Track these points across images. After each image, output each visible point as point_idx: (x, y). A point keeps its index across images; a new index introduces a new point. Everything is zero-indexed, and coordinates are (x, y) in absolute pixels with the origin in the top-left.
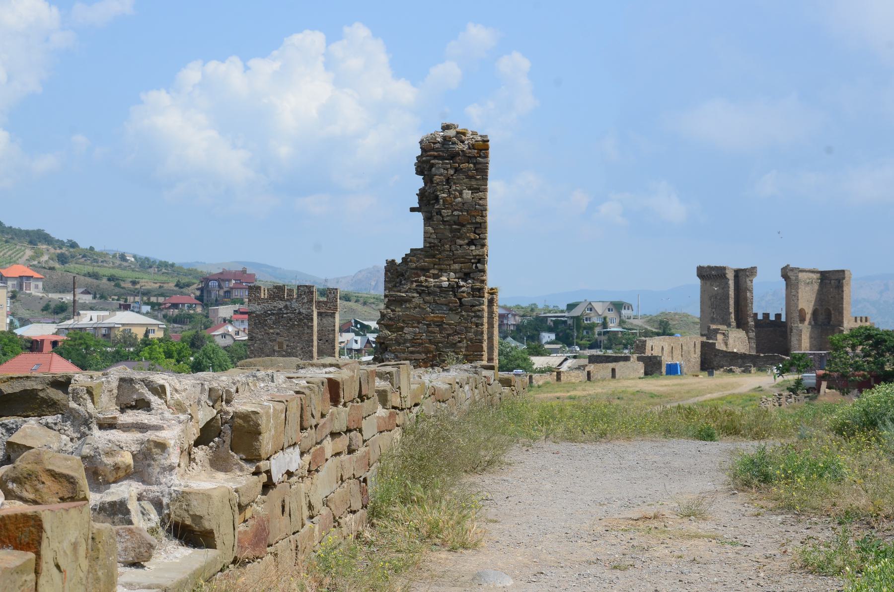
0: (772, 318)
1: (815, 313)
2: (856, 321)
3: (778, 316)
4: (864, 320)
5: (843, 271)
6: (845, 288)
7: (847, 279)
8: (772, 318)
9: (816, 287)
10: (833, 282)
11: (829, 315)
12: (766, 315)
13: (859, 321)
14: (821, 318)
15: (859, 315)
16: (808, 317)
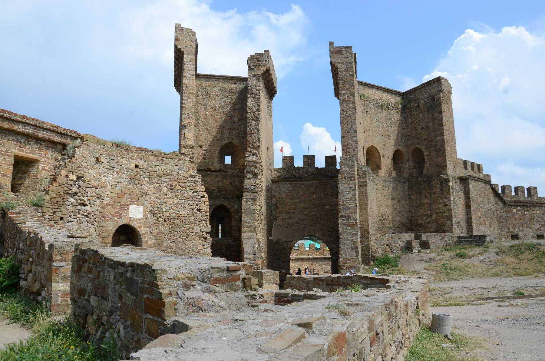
0: (320, 163)
1: (397, 157)
2: (466, 167)
3: (330, 160)
4: (476, 169)
5: (438, 79)
6: (444, 108)
7: (445, 92)
8: (320, 163)
9: (396, 116)
10: (421, 102)
11: (419, 157)
12: (309, 160)
13: (470, 169)
14: (407, 166)
15: (471, 159)
16: (386, 162)
